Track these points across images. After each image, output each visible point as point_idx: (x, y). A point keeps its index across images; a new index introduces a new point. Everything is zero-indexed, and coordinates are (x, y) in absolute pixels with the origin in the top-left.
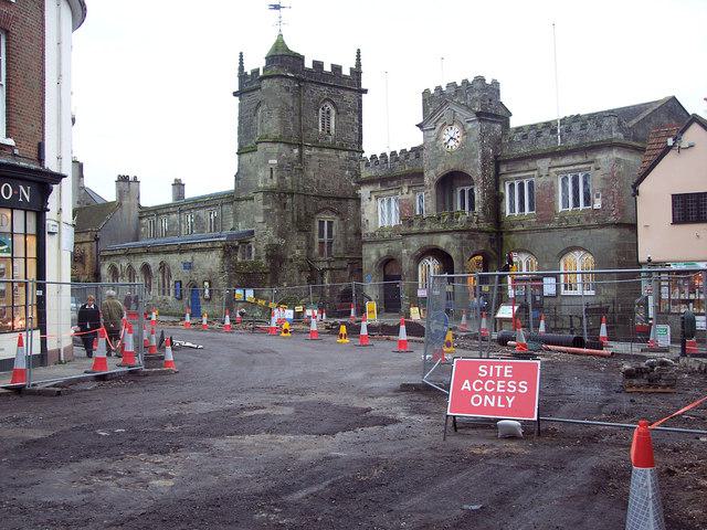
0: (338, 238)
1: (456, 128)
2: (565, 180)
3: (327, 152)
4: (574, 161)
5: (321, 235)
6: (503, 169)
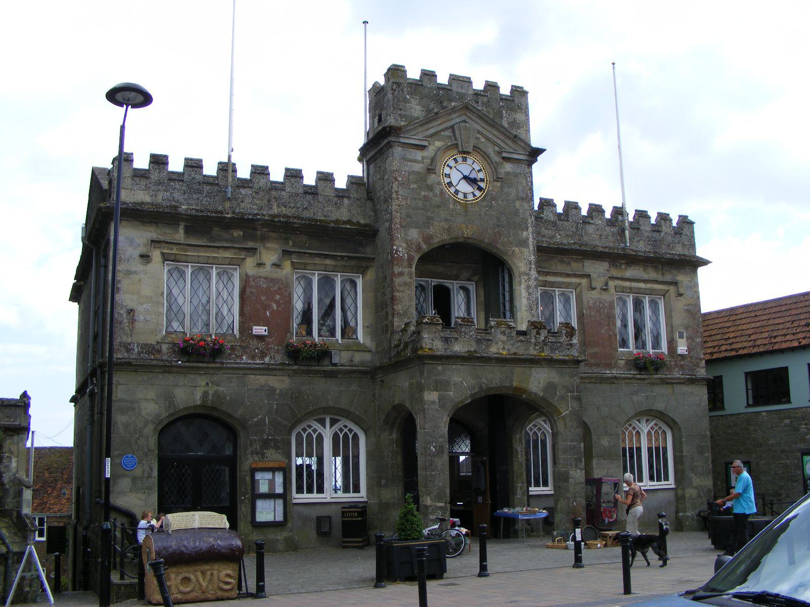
4: (646, 276)
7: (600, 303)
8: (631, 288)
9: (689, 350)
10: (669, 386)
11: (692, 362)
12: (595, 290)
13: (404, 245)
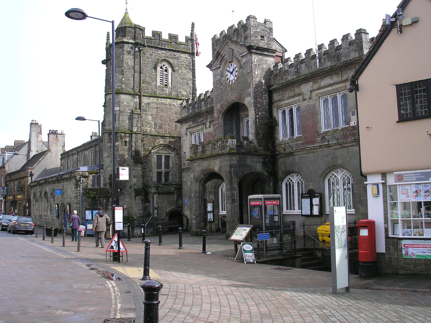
0: (175, 170)
1: (234, 65)
2: (326, 101)
3: (163, 101)
4: (332, 82)
6: (276, 97)
8: (324, 92)
10: (345, 149)
12: (306, 101)
13: (216, 112)
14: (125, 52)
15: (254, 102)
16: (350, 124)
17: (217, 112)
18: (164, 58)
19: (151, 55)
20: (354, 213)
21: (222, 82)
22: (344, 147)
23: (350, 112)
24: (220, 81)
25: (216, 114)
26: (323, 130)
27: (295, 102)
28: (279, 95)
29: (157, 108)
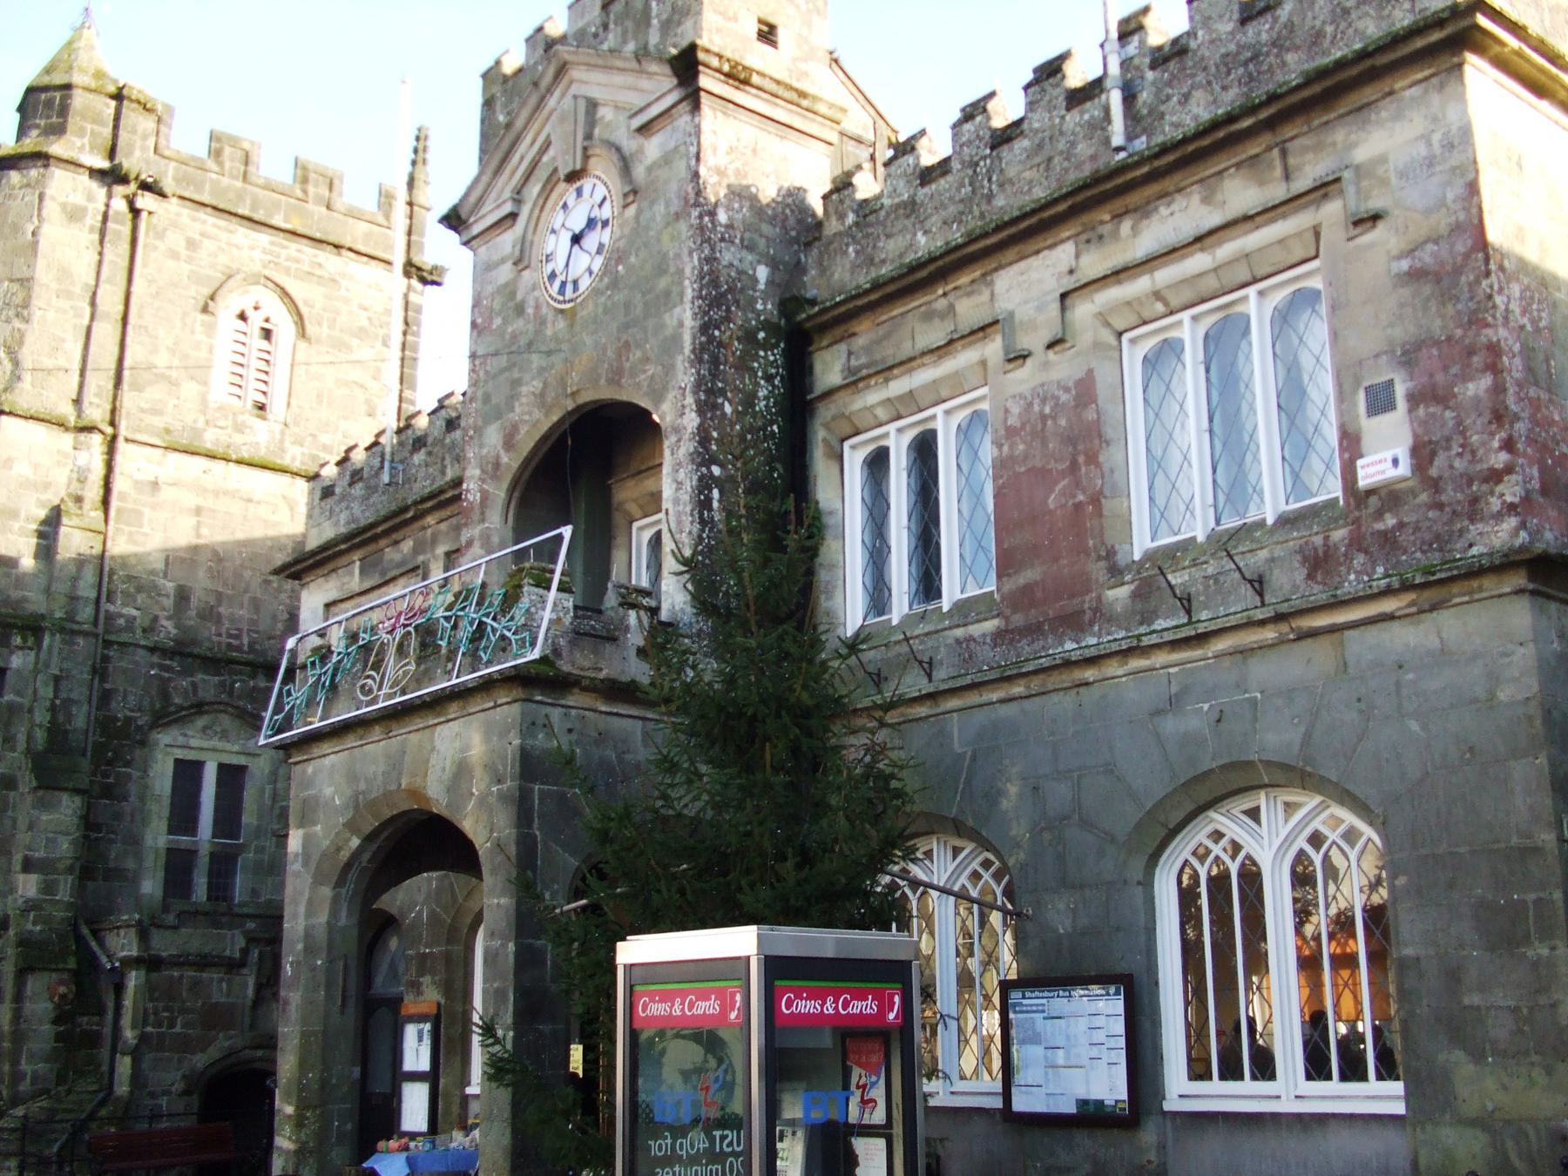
2: (1164, 356)
4: (1214, 219)
5: (184, 815)
6: (829, 368)
7: (1044, 401)
8: (1157, 295)
9: (1422, 453)
10: (1324, 642)
11: (1440, 506)
12: (1029, 361)
14: (50, 208)
15: (699, 384)
16: (1361, 473)
17: (483, 471)
18: (257, 268)
19: (191, 244)
20: (1399, 1108)
21: (519, 297)
22: (1314, 633)
23: (1355, 392)
24: (509, 291)
25: (472, 489)
26: (1141, 542)
27: (958, 384)
28: (850, 353)
29: (198, 511)
